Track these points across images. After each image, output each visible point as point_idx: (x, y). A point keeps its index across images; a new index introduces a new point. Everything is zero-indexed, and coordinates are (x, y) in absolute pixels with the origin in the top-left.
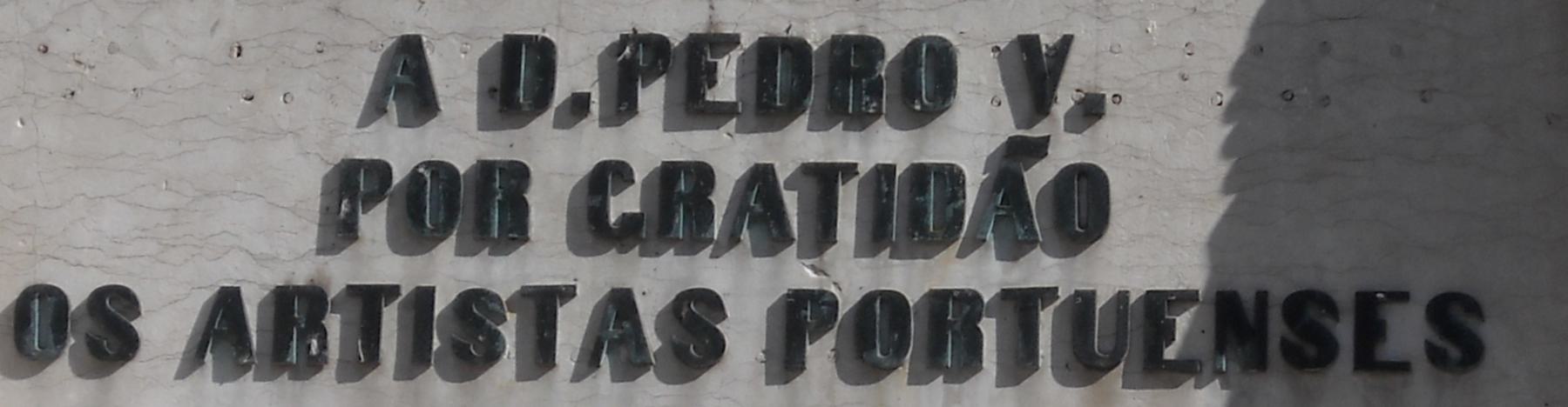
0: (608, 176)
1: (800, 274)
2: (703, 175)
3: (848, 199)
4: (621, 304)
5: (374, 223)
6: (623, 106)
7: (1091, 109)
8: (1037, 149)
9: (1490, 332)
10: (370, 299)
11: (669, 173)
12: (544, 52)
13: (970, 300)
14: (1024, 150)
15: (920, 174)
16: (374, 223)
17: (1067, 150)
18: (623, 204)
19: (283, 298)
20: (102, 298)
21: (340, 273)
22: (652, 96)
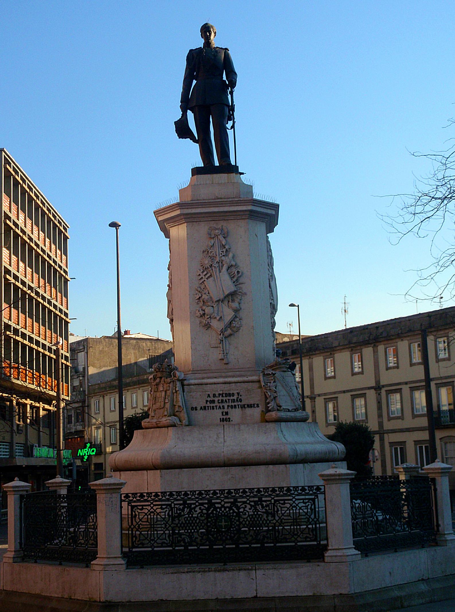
0: (219, 400)
1: (228, 404)
2: (223, 400)
3: (230, 401)
4: (220, 406)
5: (208, 403)
6: (219, 397)
7: (241, 396)
8: (238, 398)
9: (259, 405)
10: (208, 407)
11: (221, 400)
12: (215, 395)
13: (236, 405)
14: (237, 398)
15: (233, 399)
16: (208, 403)
17: (240, 397)
18: (219, 401)
19: (204, 407)
20: (195, 407)
21: (206, 405)
22: (221, 396)
